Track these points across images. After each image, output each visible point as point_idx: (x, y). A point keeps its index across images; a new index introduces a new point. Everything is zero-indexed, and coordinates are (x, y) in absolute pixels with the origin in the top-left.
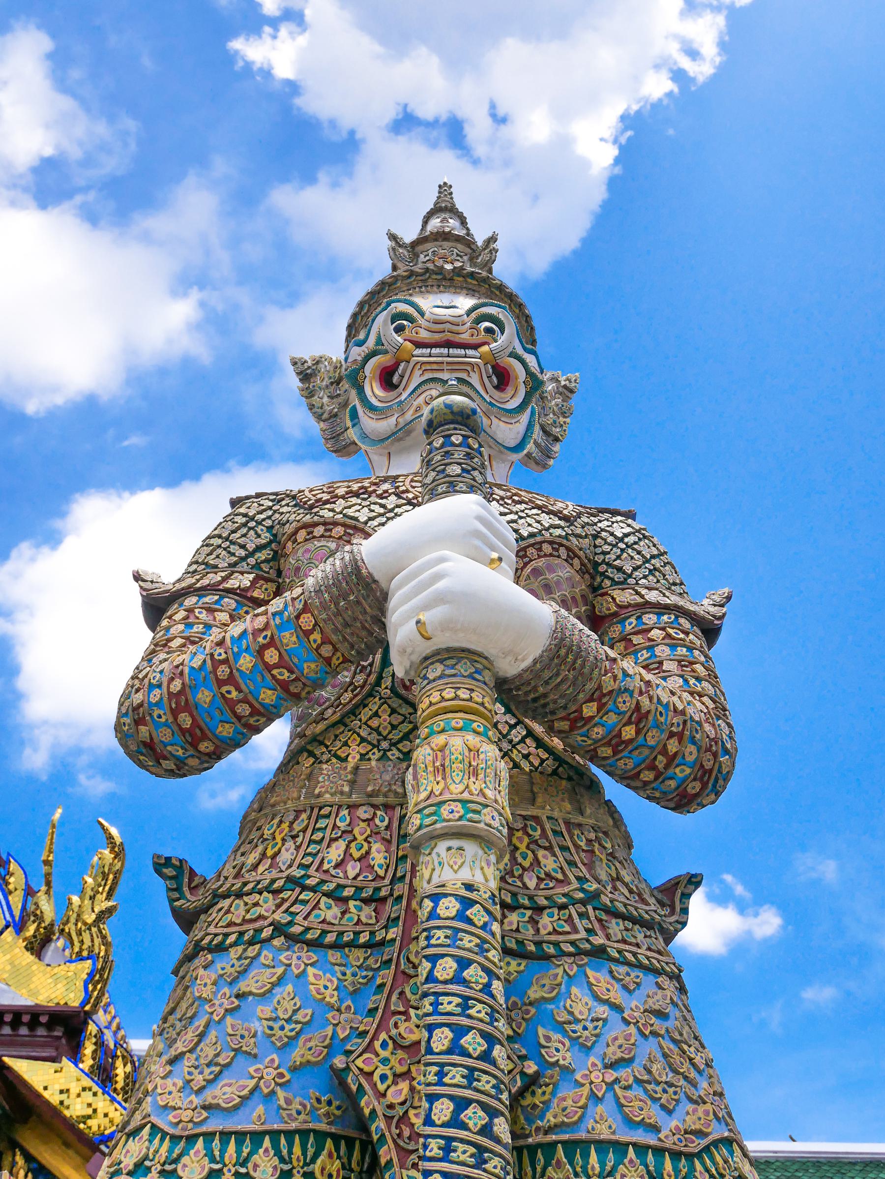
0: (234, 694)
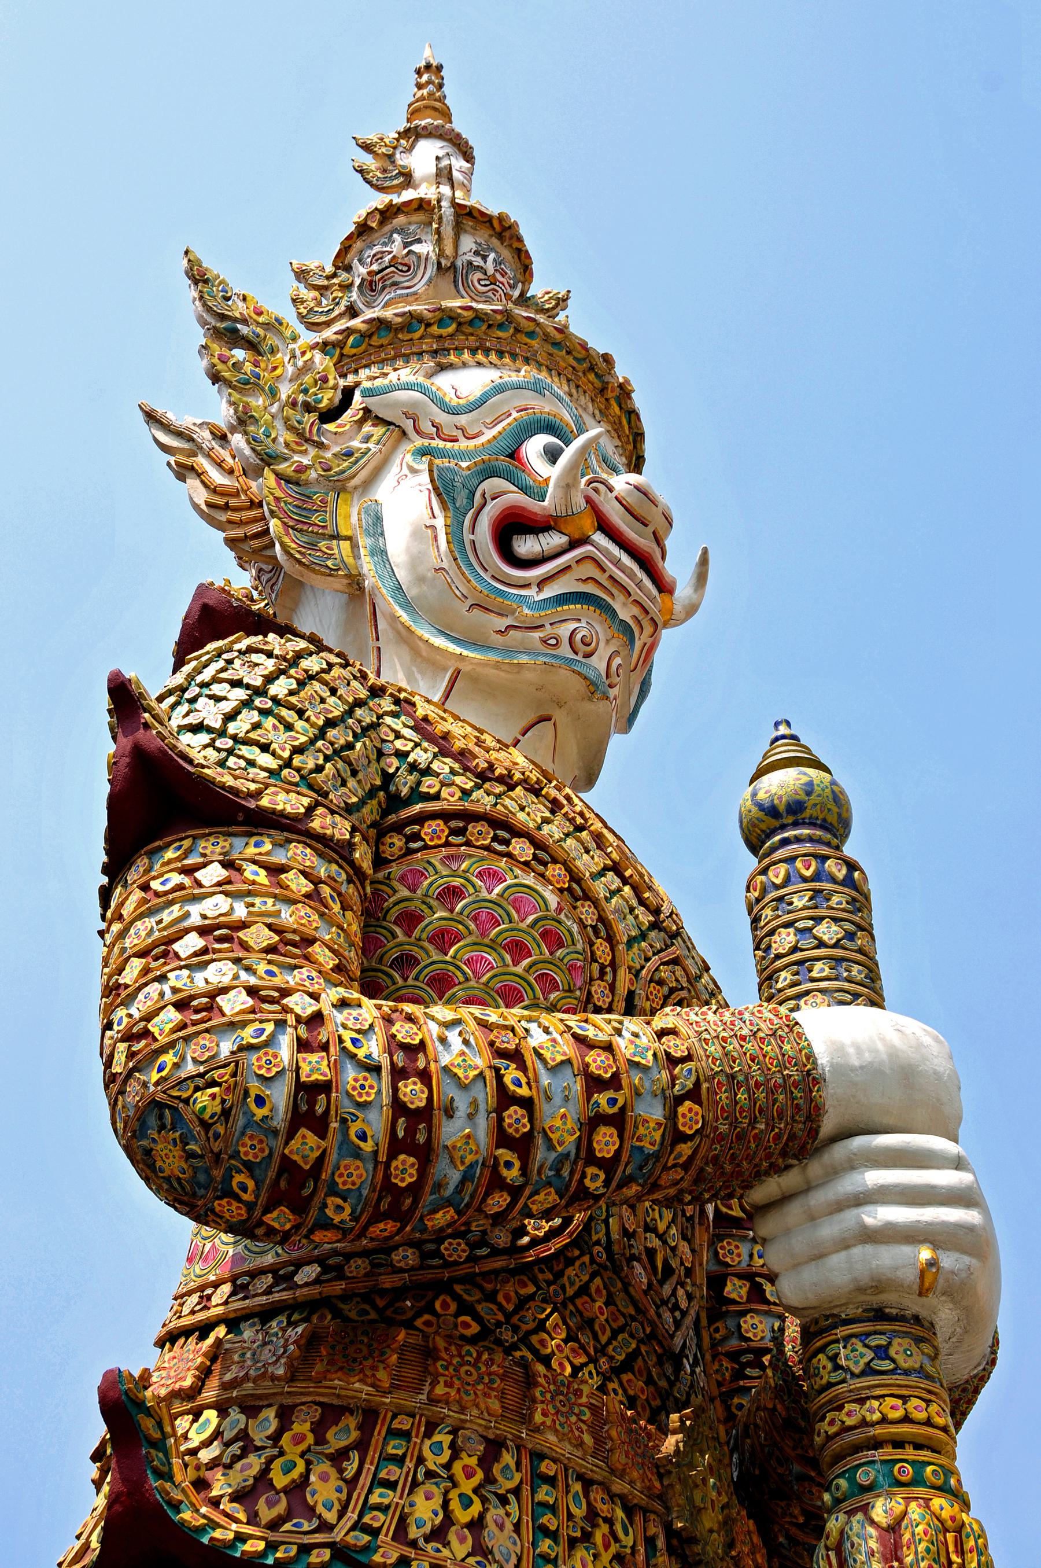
0: (512, 1175)
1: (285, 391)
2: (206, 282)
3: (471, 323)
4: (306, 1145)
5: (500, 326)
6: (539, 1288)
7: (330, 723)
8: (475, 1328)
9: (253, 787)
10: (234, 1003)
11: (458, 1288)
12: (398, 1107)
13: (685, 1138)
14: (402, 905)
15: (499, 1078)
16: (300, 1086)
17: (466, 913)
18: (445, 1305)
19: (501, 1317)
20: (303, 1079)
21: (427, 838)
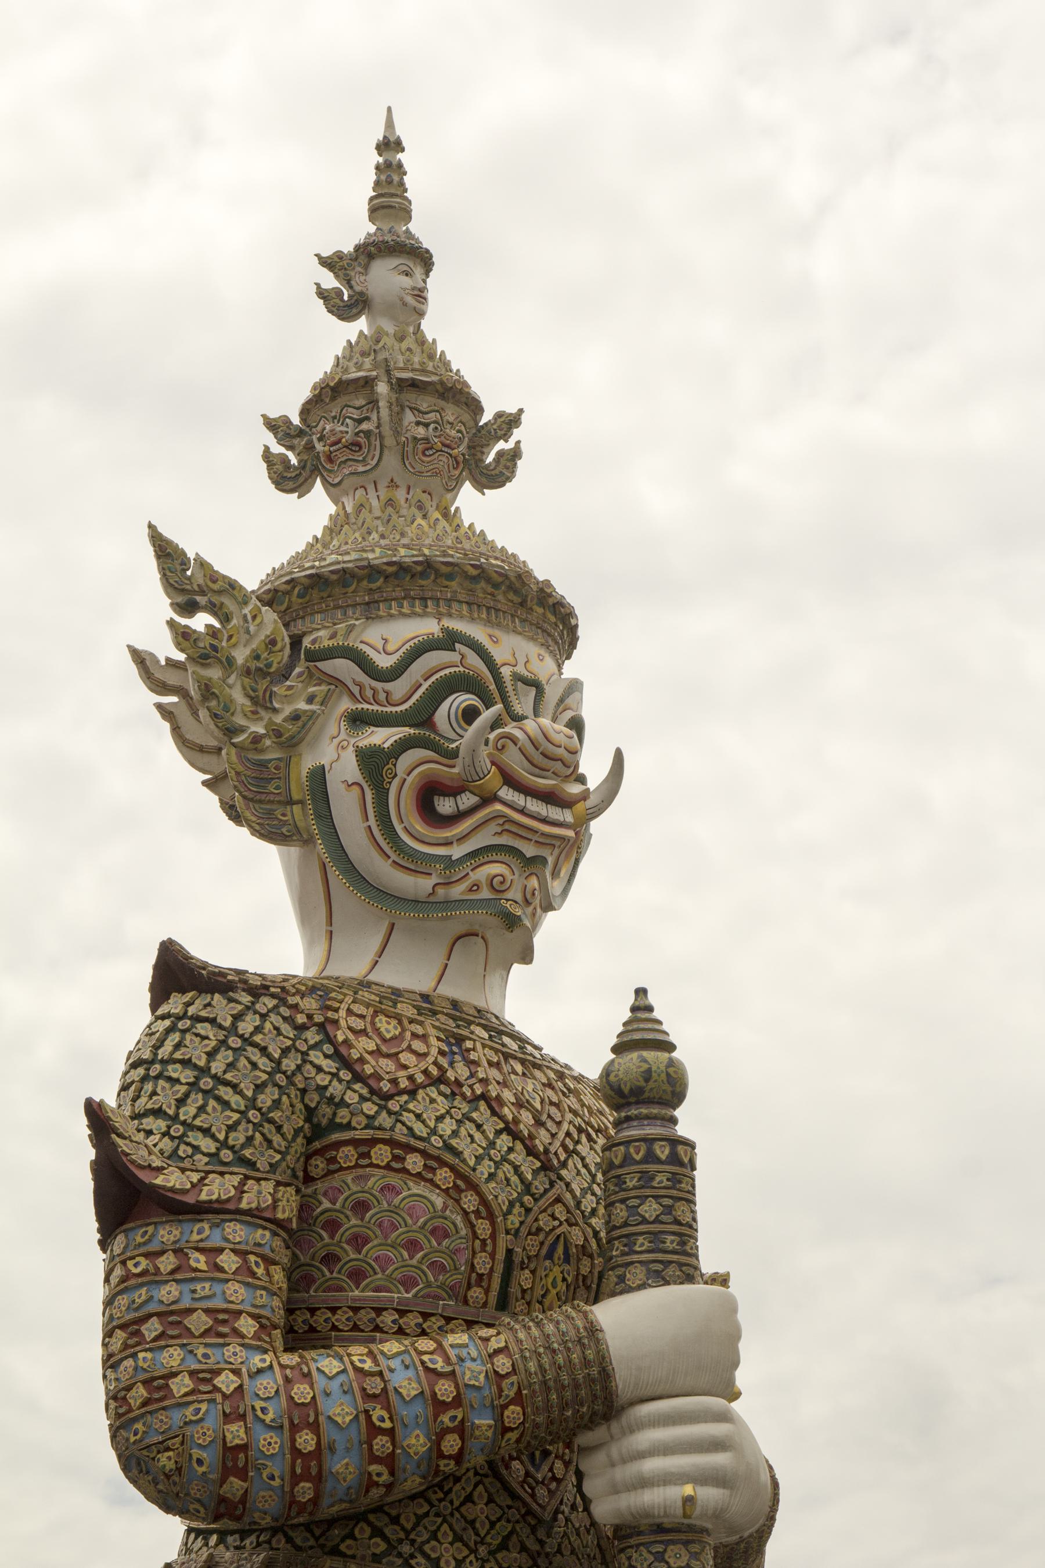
1: (241, 656)
2: (168, 555)
3: (396, 575)
4: (235, 1486)
5: (423, 575)
6: (432, 1505)
7: (259, 1088)
8: (383, 1546)
9: (195, 1177)
10: (181, 1385)
11: (371, 1517)
12: (296, 1452)
13: (511, 1429)
14: (326, 1215)
15: (369, 1417)
16: (226, 1448)
17: (373, 1221)
18: (362, 1530)
19: (402, 1535)
20: (229, 1445)
21: (341, 1161)
